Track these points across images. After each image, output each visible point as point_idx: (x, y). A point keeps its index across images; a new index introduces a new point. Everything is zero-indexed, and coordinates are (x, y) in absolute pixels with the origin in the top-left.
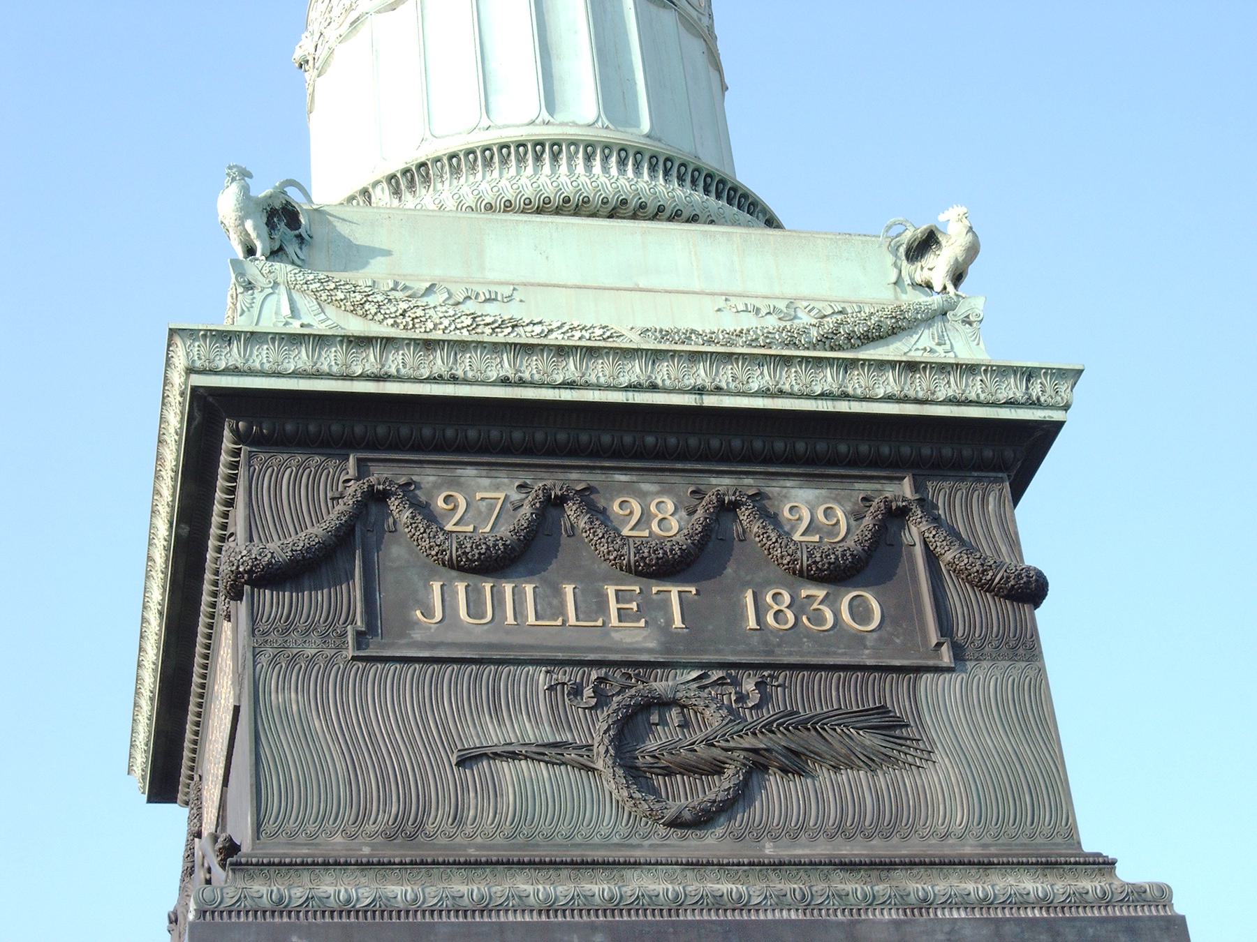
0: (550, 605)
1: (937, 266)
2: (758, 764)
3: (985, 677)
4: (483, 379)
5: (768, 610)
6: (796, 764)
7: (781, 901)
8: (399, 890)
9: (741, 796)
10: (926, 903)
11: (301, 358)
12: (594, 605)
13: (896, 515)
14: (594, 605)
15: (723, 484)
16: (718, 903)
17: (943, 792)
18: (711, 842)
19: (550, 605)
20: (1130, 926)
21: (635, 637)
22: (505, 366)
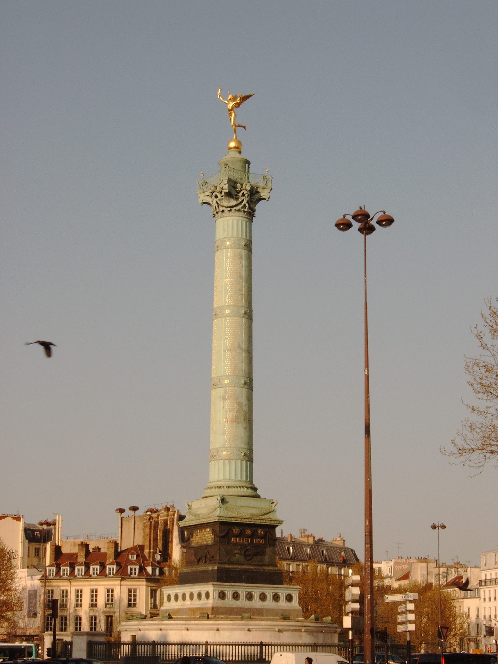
0: (240, 540)
1: (273, 505)
2: (253, 556)
3: (271, 548)
4: (239, 521)
5: (255, 541)
6: (256, 555)
7: (255, 569)
8: (230, 567)
9: (252, 558)
10: (264, 570)
11: (226, 519)
12: (243, 540)
13: (266, 532)
14: (243, 540)
15: (254, 529)
16: (251, 569)
17: (267, 559)
18: (250, 561)
19: (240, 540)
20: (279, 573)
21: (246, 543)
22: (240, 520)
